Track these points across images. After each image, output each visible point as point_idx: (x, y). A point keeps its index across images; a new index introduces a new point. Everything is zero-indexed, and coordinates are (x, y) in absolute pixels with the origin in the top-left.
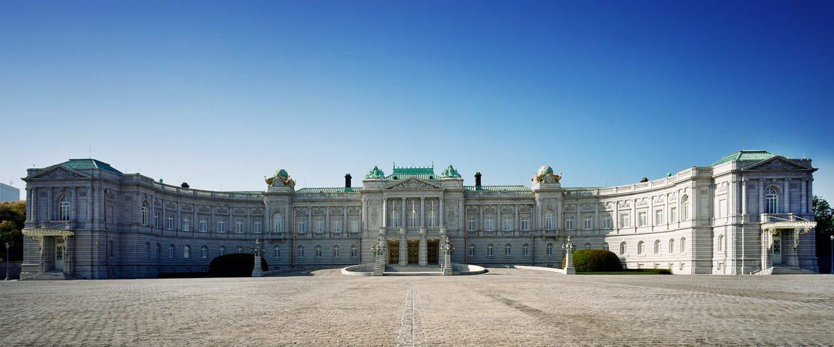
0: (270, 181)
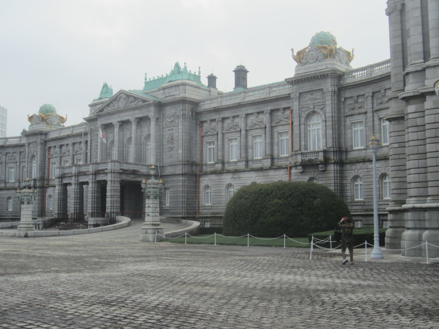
0: (31, 119)
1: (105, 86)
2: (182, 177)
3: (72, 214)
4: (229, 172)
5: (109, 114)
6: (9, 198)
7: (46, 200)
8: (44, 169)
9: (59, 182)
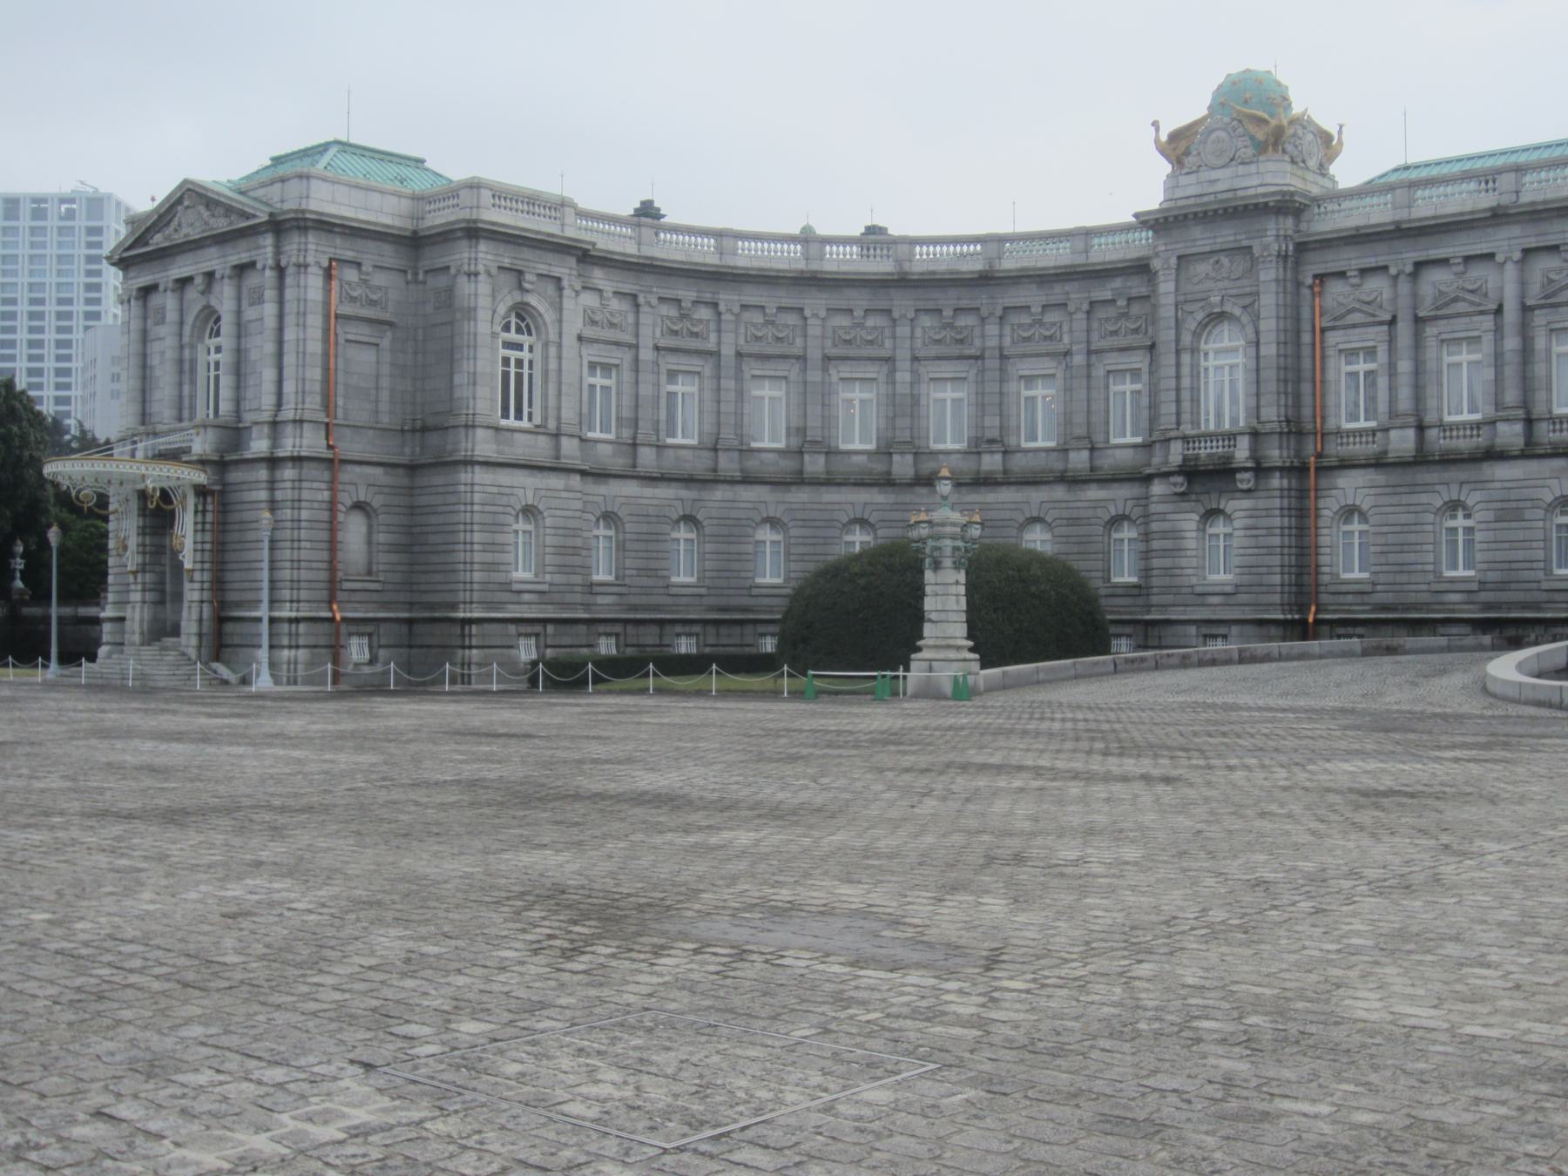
6: (1116, 521)
8: (1298, 381)
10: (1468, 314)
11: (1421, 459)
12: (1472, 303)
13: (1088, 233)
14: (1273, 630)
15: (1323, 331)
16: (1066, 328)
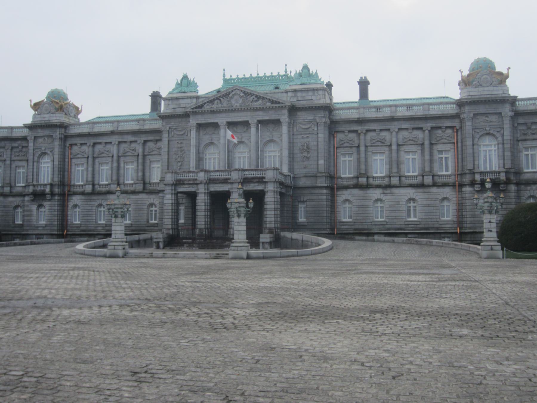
0: (36, 106)
1: (185, 77)
2: (326, 190)
3: (201, 229)
4: (378, 187)
5: (213, 112)
7: (69, 211)
8: (64, 171)
9: (172, 190)
10: (106, 157)
11: (94, 193)
12: (107, 154)
13: (12, 128)
14: (55, 237)
15: (71, 159)
16: (5, 153)
